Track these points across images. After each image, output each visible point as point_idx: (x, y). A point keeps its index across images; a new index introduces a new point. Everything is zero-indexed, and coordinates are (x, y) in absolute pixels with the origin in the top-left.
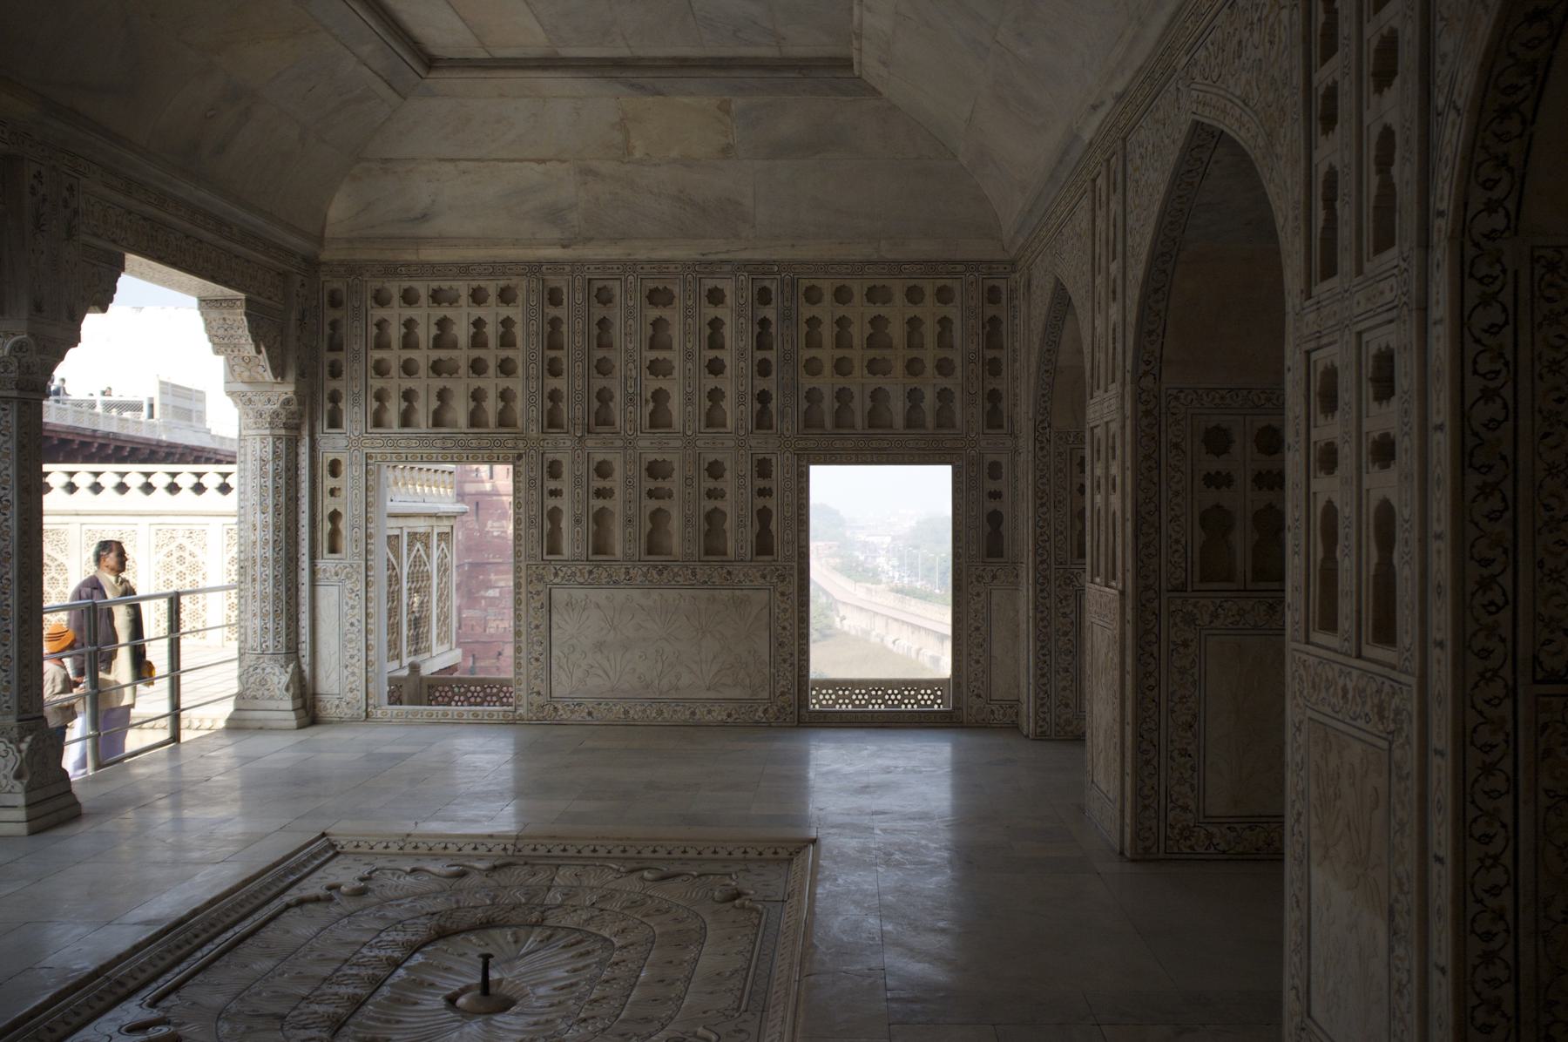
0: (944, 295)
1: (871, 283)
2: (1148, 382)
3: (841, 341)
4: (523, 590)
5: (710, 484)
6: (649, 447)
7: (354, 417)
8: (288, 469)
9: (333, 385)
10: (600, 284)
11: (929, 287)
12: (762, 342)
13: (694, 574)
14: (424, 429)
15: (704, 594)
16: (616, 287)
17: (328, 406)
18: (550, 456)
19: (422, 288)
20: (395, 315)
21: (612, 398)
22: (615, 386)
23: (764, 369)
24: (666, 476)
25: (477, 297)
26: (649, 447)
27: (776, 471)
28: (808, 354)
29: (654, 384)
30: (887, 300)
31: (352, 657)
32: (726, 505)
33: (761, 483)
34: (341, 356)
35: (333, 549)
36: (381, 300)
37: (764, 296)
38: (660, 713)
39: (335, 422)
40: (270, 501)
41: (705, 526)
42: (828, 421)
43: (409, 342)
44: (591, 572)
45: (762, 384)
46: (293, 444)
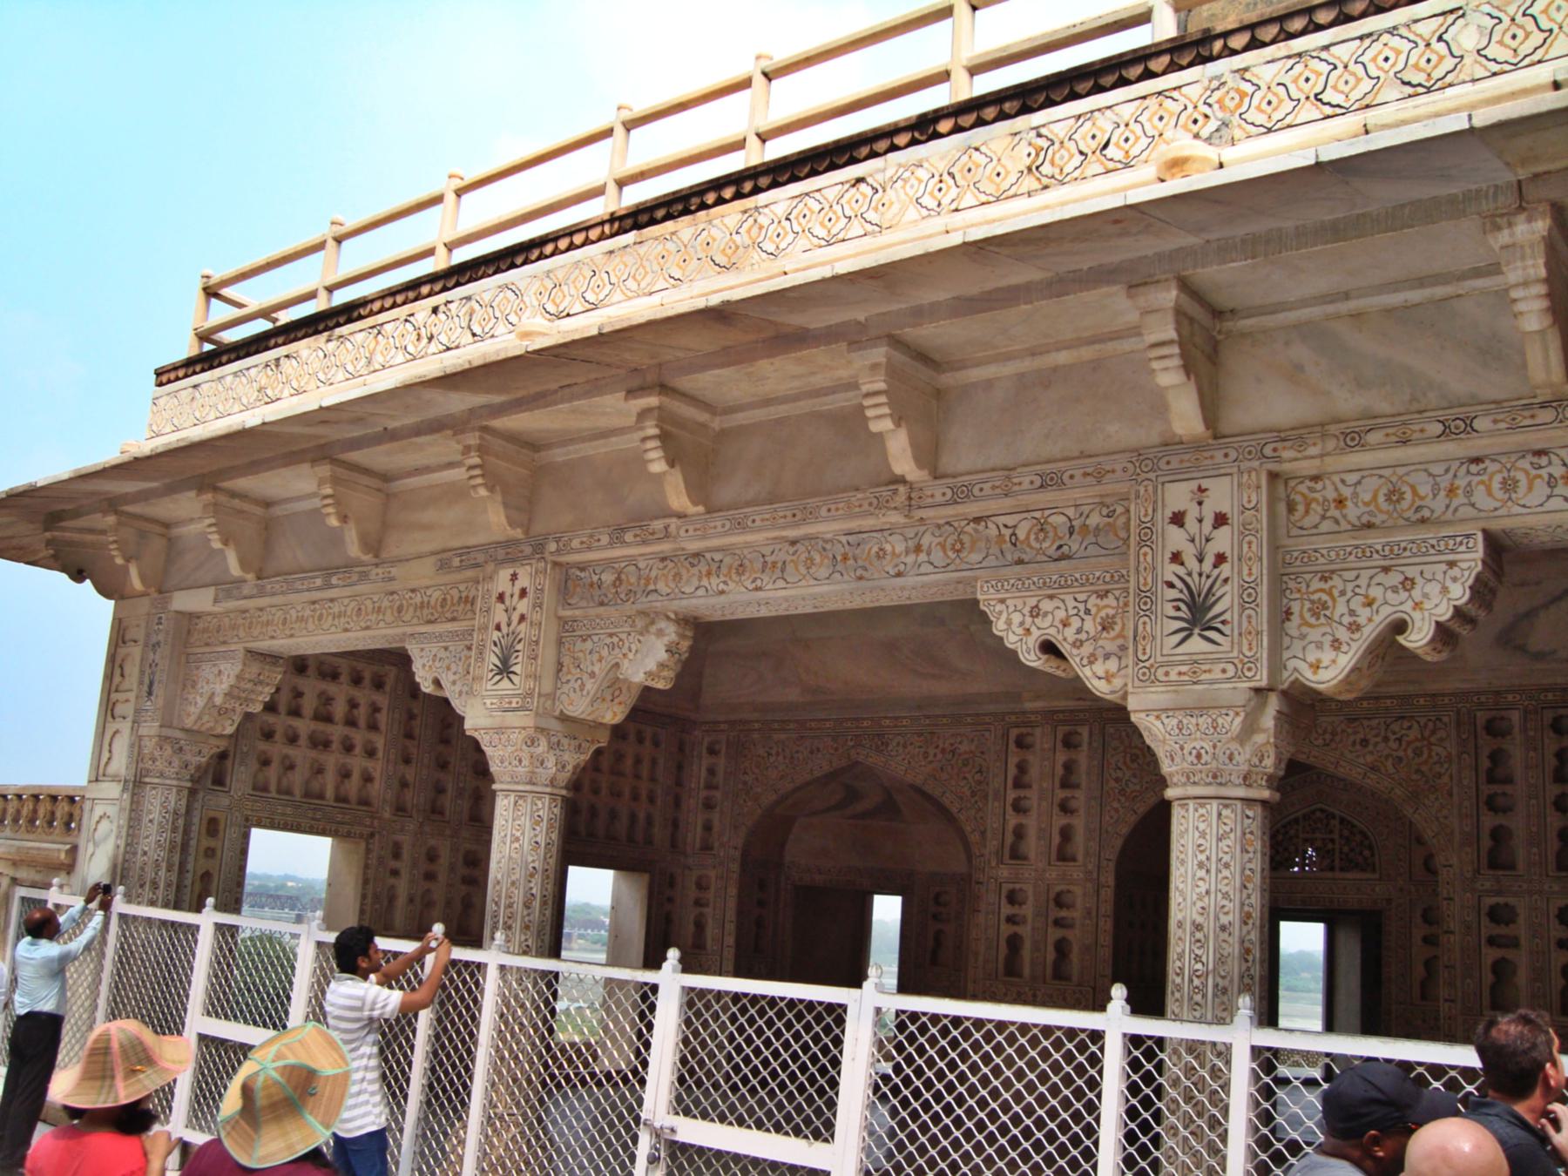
14: (298, 798)
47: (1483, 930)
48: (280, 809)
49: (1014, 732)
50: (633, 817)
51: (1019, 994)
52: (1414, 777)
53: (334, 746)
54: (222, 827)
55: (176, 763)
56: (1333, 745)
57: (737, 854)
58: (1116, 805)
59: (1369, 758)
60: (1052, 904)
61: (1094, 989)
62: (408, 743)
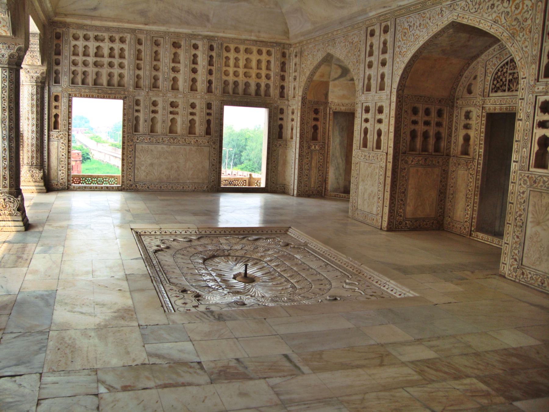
0: (269, 53)
1: (246, 47)
2: (400, 92)
3: (236, 66)
4: (126, 144)
5: (191, 110)
6: (171, 97)
7: (65, 80)
8: (41, 98)
9: (56, 68)
10: (155, 39)
11: (264, 50)
12: (210, 63)
13: (185, 140)
14: (91, 85)
15: (188, 148)
16: (161, 40)
17: (54, 75)
18: (137, 98)
19: (91, 34)
20: (81, 43)
21: (158, 79)
22: (160, 75)
23: (210, 72)
24: (177, 106)
25: (86, 38)
26: (171, 97)
27: (214, 107)
28: (224, 69)
29: (173, 75)
30: (251, 53)
31: (62, 167)
32: (196, 118)
33: (208, 111)
34: (60, 57)
35: (56, 127)
36: (76, 38)
37: (211, 48)
38: (172, 187)
39: (57, 81)
40: (35, 110)
41: (189, 125)
42: (231, 91)
43: (85, 54)
44: (150, 139)
45: (210, 78)
46: (43, 89)
47: (536, 118)
48: (83, 90)
49: (369, 29)
50: (258, 86)
51: (365, 156)
52: (514, 23)
53: (105, 66)
54: (60, 98)
55: (28, 77)
56: (479, 11)
57: (300, 98)
58: (398, 60)
59: (494, 15)
60: (377, 112)
61: (387, 154)
62: (138, 62)
